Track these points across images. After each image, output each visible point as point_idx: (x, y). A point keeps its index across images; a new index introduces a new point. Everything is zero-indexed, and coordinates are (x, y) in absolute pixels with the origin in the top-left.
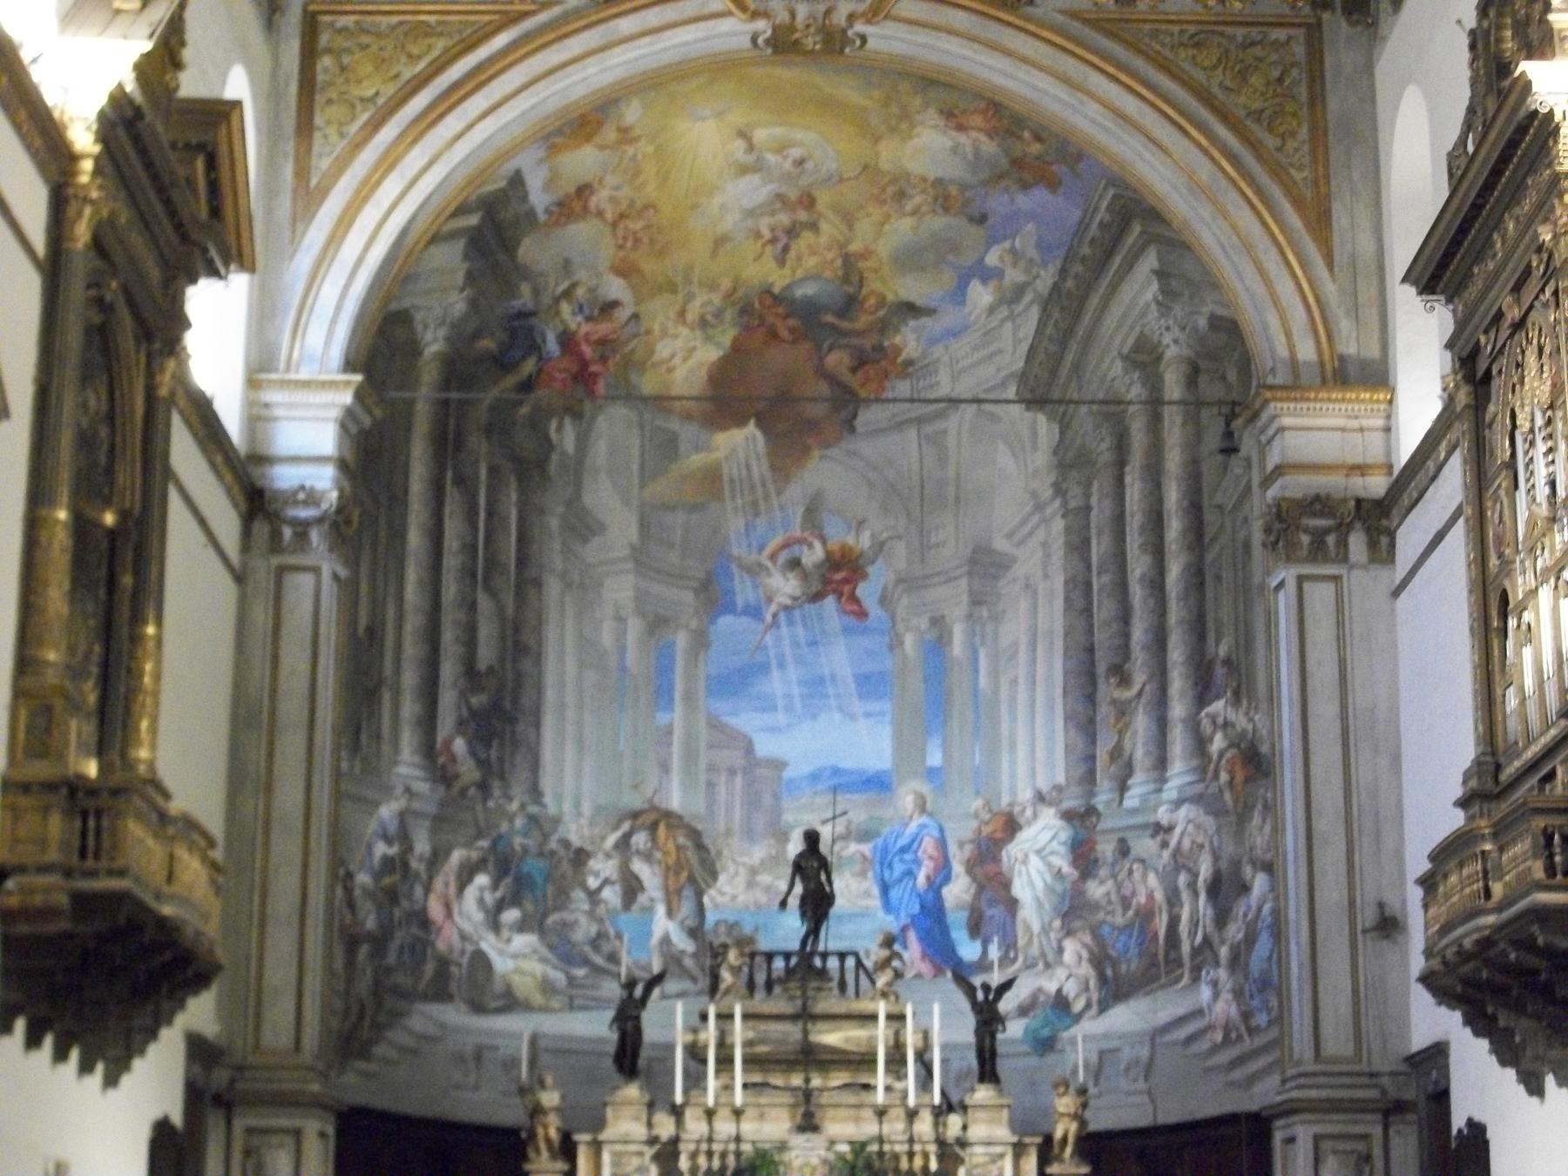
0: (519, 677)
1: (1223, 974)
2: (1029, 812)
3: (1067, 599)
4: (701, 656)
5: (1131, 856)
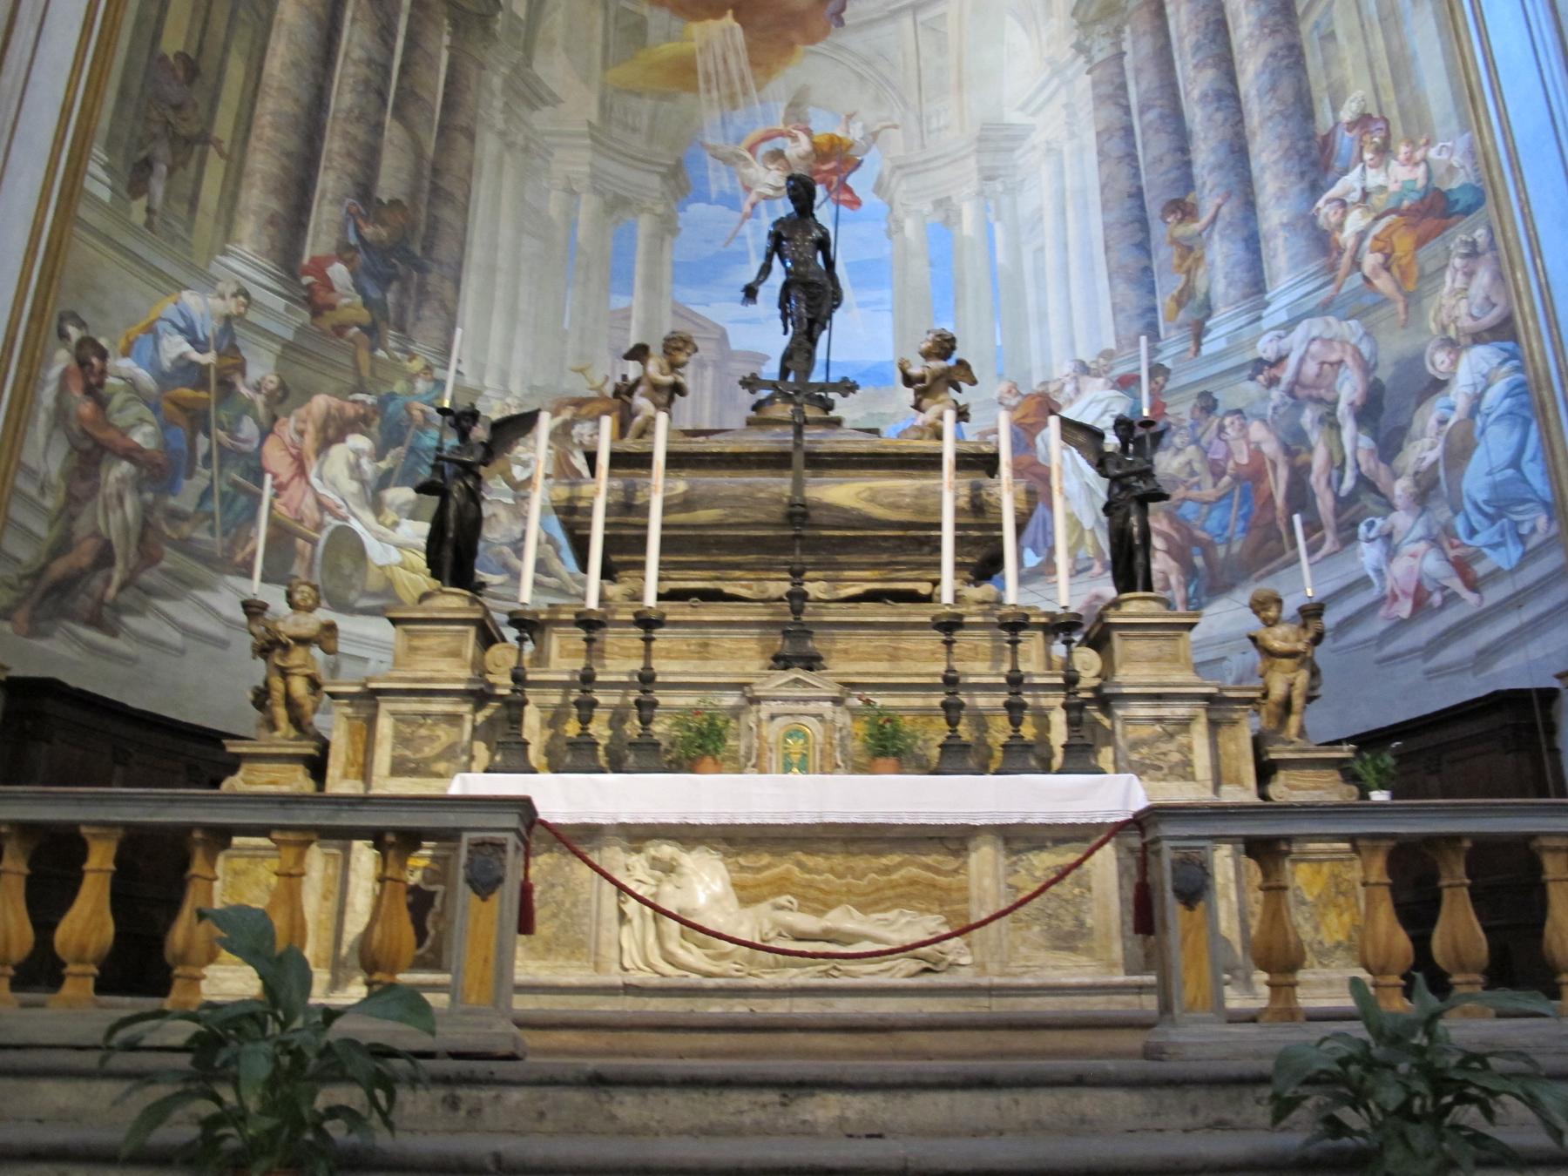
0: (434, 224)
1: (1401, 520)
2: (1069, 388)
3: (1100, 152)
5: (1220, 411)
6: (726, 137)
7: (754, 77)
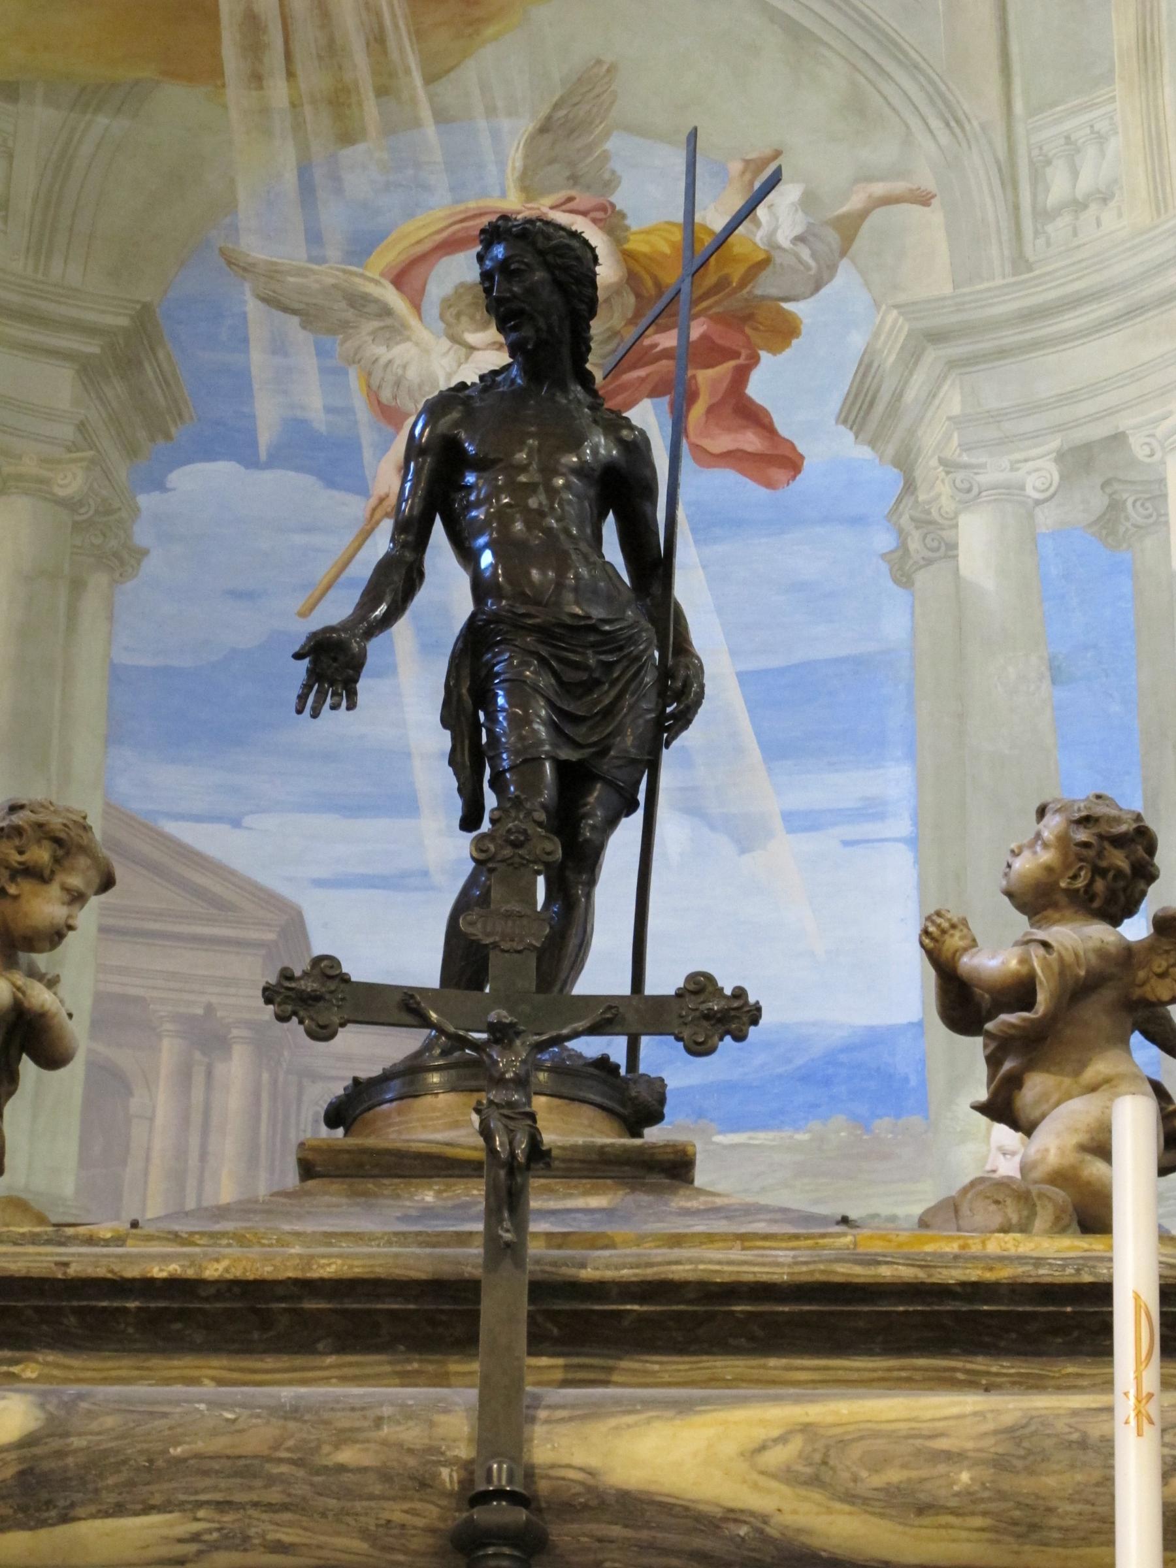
4: (91, 604)
6: (314, 237)
7: (419, 34)
